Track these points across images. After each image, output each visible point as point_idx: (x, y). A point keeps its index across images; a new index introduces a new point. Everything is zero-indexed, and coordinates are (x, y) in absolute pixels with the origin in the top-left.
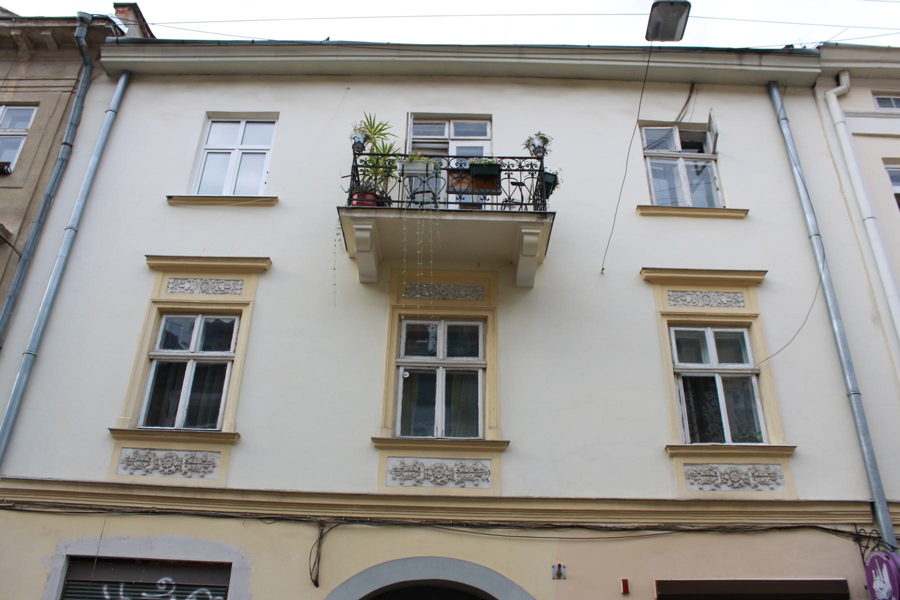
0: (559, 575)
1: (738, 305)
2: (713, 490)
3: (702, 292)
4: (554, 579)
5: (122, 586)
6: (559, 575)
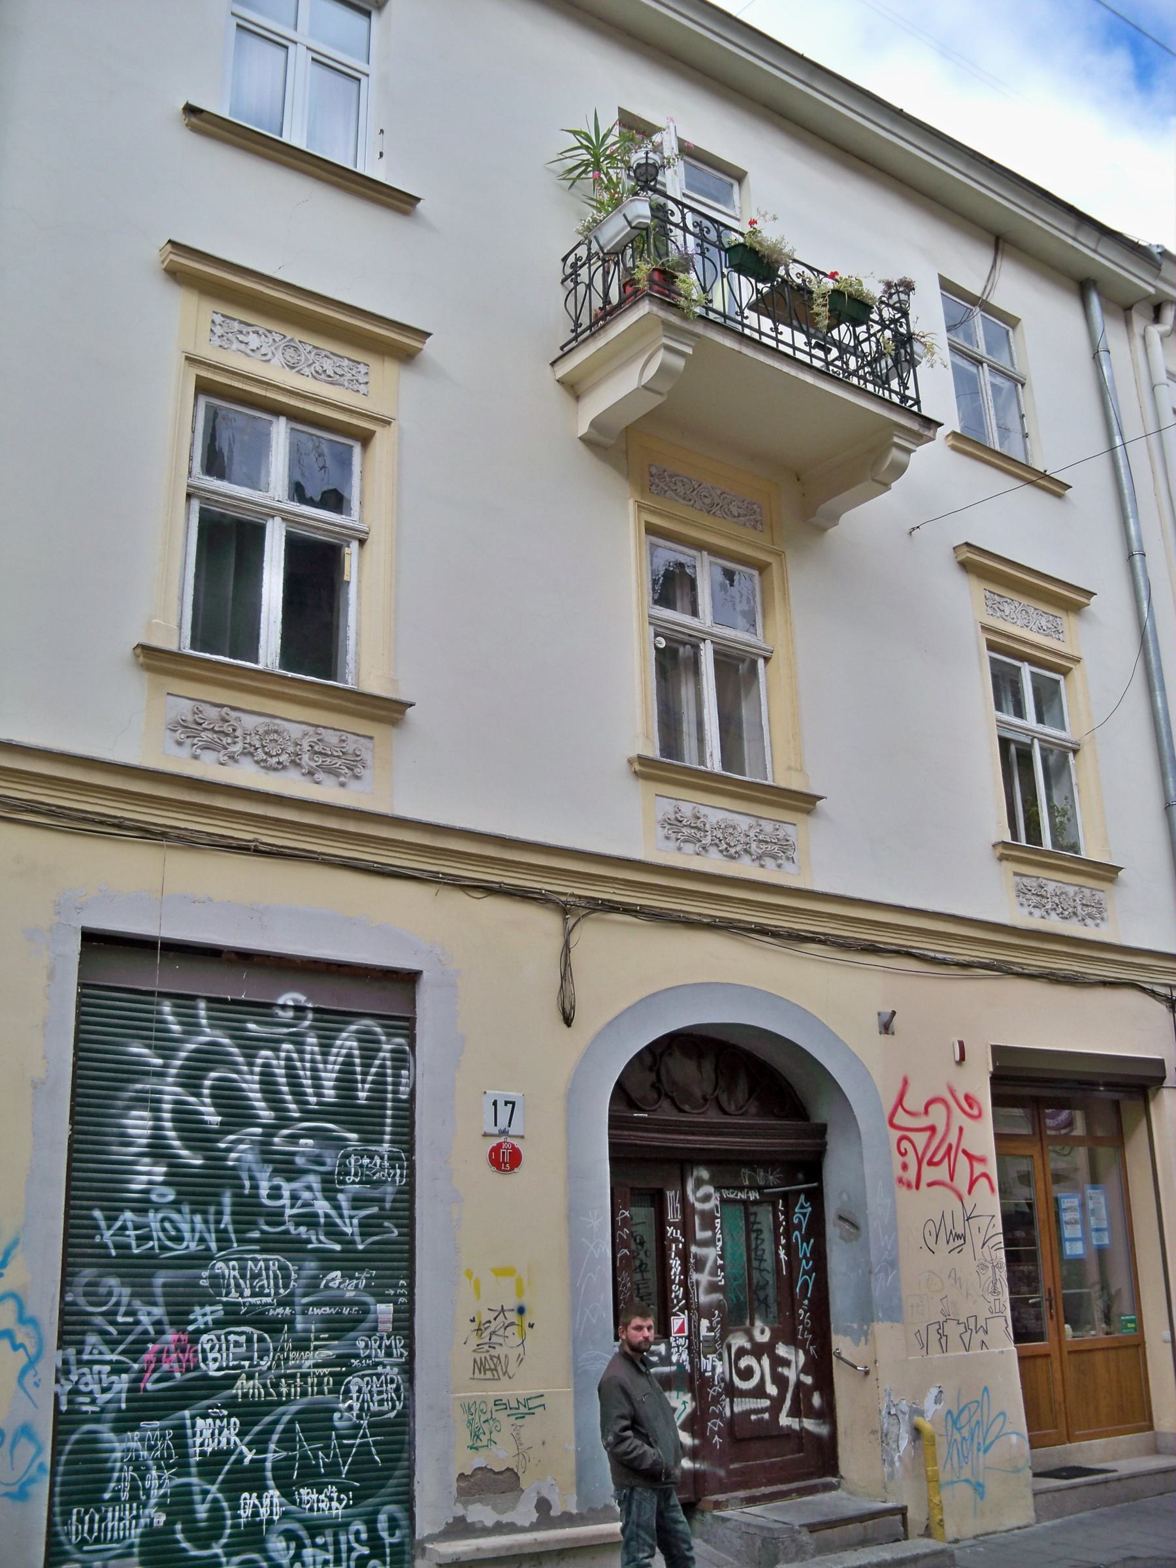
0: (886, 1027)
4: (881, 1033)
5: (202, 1004)
6: (886, 1027)
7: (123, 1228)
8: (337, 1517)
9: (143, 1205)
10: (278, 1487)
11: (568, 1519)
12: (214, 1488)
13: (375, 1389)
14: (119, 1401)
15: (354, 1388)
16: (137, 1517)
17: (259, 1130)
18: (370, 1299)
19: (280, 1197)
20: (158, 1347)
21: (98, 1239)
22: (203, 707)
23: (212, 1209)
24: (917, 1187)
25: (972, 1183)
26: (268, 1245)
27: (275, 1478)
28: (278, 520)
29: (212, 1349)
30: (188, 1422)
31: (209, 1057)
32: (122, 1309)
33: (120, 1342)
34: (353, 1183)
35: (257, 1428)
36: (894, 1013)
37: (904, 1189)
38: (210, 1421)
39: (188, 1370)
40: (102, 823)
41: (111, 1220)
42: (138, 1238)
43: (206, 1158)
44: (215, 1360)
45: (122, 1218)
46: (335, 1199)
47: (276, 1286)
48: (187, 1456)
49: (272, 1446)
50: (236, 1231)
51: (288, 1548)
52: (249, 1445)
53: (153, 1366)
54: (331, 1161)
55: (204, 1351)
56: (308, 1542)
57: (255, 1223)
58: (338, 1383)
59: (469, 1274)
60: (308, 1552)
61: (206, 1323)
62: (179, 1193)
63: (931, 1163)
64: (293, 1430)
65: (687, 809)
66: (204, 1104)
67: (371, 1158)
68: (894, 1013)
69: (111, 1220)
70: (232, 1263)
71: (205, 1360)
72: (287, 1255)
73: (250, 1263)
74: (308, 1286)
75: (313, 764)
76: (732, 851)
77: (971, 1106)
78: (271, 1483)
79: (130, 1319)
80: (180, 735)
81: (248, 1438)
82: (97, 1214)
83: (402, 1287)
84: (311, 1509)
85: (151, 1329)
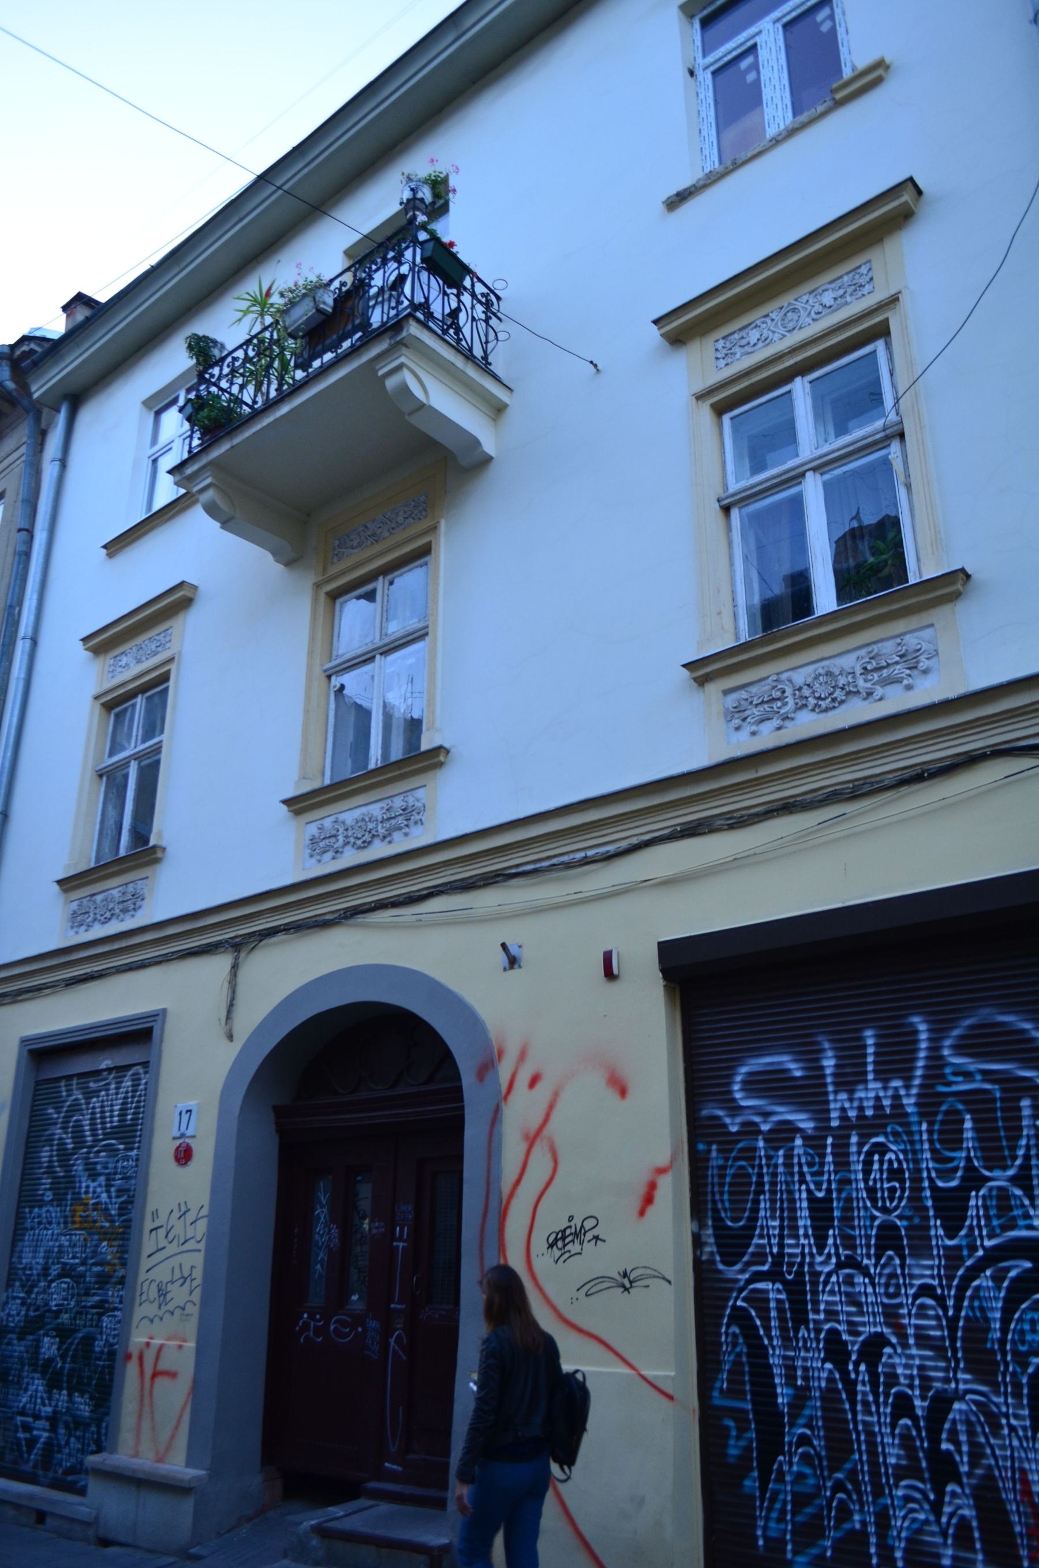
1: (860, 294)
2: (779, 728)
3: (781, 308)
23: (64, 1203)
48: (37, 1359)
62: (54, 1195)
68: (504, 946)
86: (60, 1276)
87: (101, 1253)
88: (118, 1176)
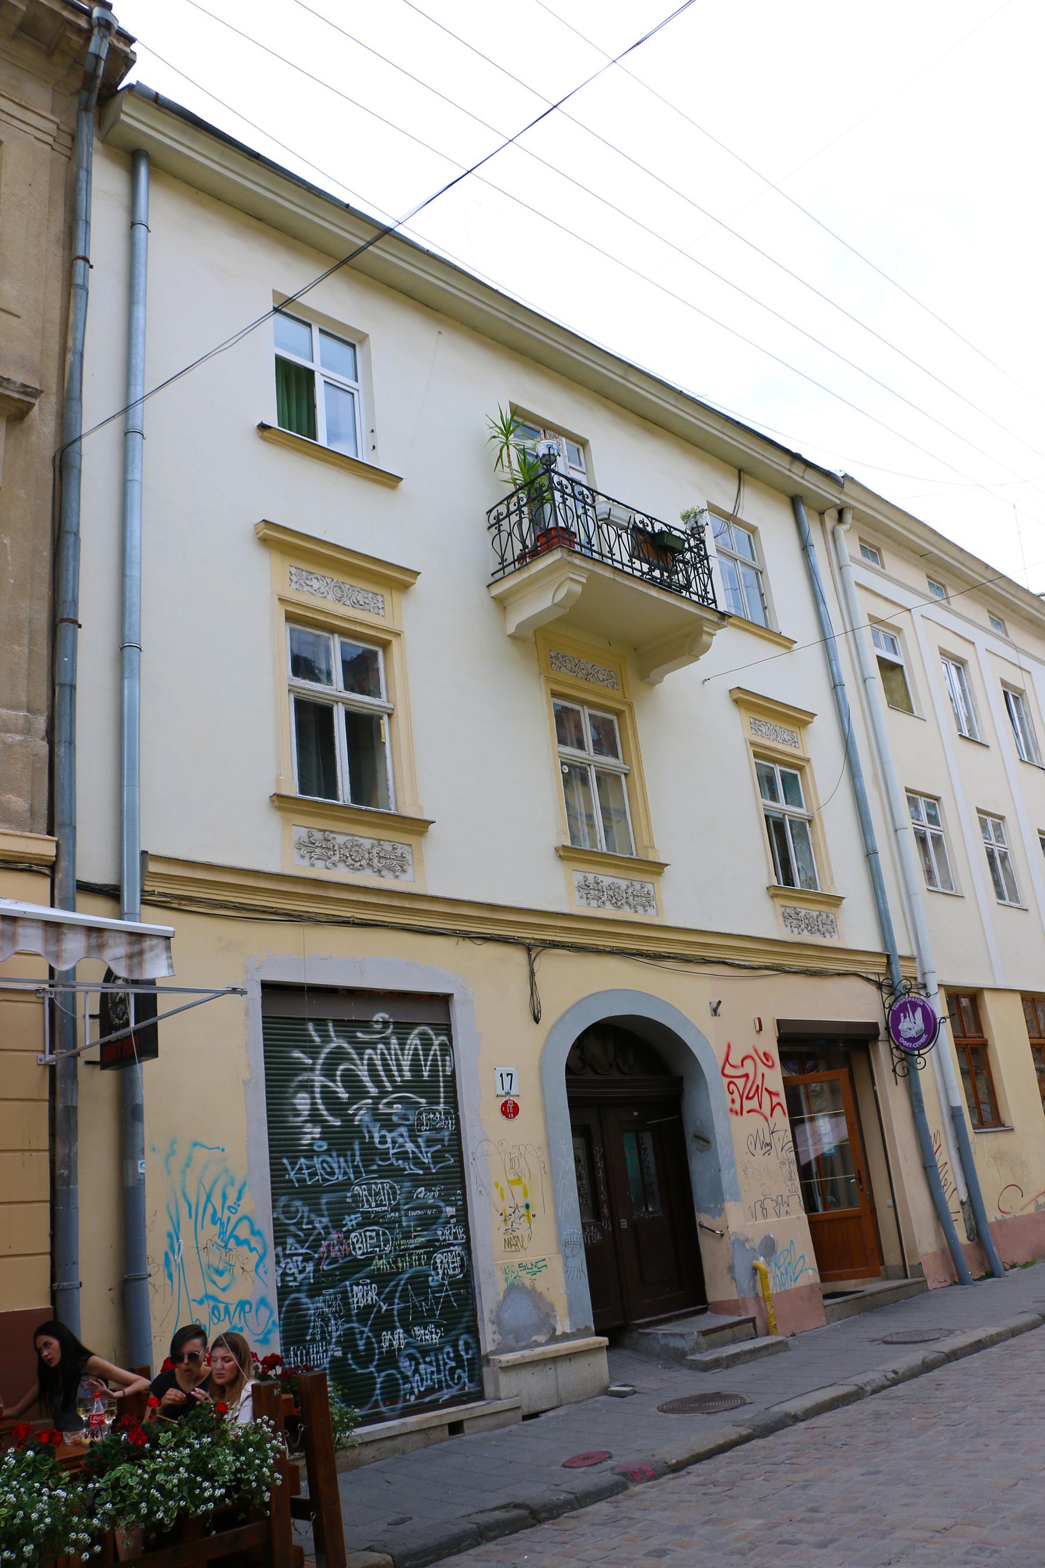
0: (715, 1011)
5: (330, 1024)
6: (715, 1011)
7: (301, 1169)
8: (436, 1344)
9: (310, 1153)
10: (402, 1327)
11: (566, 1337)
12: (366, 1330)
13: (450, 1261)
14: (309, 1279)
15: (438, 1261)
16: (326, 1351)
17: (370, 1101)
18: (442, 1204)
19: (386, 1142)
20: (327, 1242)
21: (287, 1177)
22: (315, 832)
23: (349, 1153)
24: (742, 1114)
25: (772, 1110)
26: (384, 1173)
27: (400, 1321)
28: (340, 704)
29: (358, 1241)
30: (349, 1289)
31: (337, 1057)
32: (305, 1220)
33: (306, 1241)
34: (426, 1130)
35: (387, 1290)
36: (720, 1002)
37: (734, 1115)
38: (360, 1287)
39: (346, 1256)
40: (264, 912)
41: (293, 1164)
42: (310, 1174)
43: (342, 1121)
44: (360, 1248)
45: (299, 1163)
46: (417, 1142)
47: (389, 1200)
48: (350, 1310)
49: (396, 1301)
50: (364, 1166)
51: (411, 1365)
52: (384, 1300)
53: (325, 1255)
54: (412, 1118)
55: (353, 1243)
56: (421, 1360)
57: (374, 1160)
58: (429, 1258)
59: (497, 1185)
60: (422, 1367)
61: (352, 1226)
62: (329, 1145)
63: (748, 1098)
64: (407, 1289)
65: (591, 878)
66: (338, 1087)
67: (434, 1114)
68: (720, 1002)
69: (293, 1164)
70: (363, 1187)
71: (354, 1249)
72: (394, 1179)
73: (373, 1186)
74: (406, 1198)
75: (380, 865)
76: (619, 903)
77: (768, 1060)
78: (398, 1324)
79: (310, 1226)
80: (303, 851)
81: (383, 1296)
82: (285, 1161)
83: (459, 1194)
84: (421, 1340)
85: (322, 1231)
86: (360, 1225)
87: (417, 1197)
88: (424, 1128)
